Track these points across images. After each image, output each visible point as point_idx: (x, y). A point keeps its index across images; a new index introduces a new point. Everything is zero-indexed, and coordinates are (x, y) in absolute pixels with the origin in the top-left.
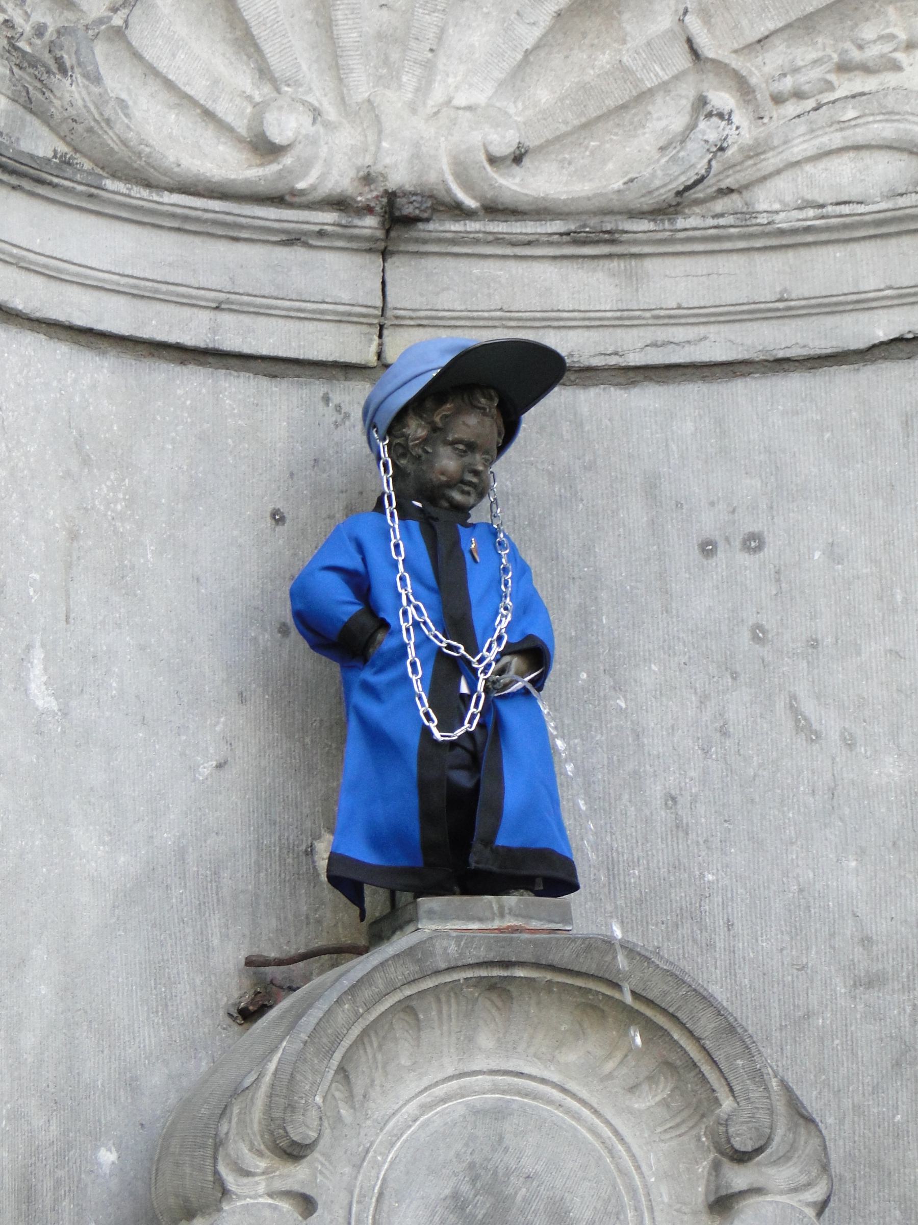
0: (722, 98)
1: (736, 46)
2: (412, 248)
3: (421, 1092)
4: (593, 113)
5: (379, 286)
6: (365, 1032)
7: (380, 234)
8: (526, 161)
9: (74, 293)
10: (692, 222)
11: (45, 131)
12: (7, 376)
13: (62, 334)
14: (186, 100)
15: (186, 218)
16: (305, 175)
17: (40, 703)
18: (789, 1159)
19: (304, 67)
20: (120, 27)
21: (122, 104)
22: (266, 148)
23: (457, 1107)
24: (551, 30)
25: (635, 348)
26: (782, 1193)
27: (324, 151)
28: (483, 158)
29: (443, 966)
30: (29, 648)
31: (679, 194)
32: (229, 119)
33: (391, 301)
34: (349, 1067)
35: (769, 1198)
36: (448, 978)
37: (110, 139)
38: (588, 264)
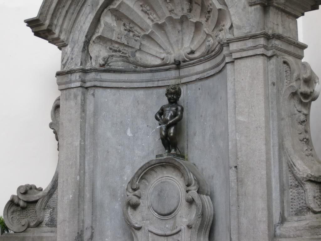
0: (210, 38)
1: (212, 31)
2: (181, 68)
3: (156, 180)
4: (200, 44)
5: (179, 73)
6: (145, 174)
7: (177, 67)
8: (195, 53)
9: (135, 84)
10: (207, 56)
11: (131, 64)
12: (124, 96)
13: (135, 89)
14: (153, 56)
15: (151, 71)
16: (167, 61)
17: (129, 135)
18: (195, 185)
19: (168, 47)
20: (139, 49)
21: (141, 59)
22: (163, 59)
23: (160, 182)
24: (194, 35)
25: (205, 75)
26: (194, 190)
27: (169, 58)
28: (187, 54)
29: (153, 164)
30: (127, 129)
31: (208, 53)
32: (159, 56)
33: (180, 75)
34: (146, 178)
35: (192, 191)
36: (155, 165)
37: (139, 63)
38: (200, 65)
